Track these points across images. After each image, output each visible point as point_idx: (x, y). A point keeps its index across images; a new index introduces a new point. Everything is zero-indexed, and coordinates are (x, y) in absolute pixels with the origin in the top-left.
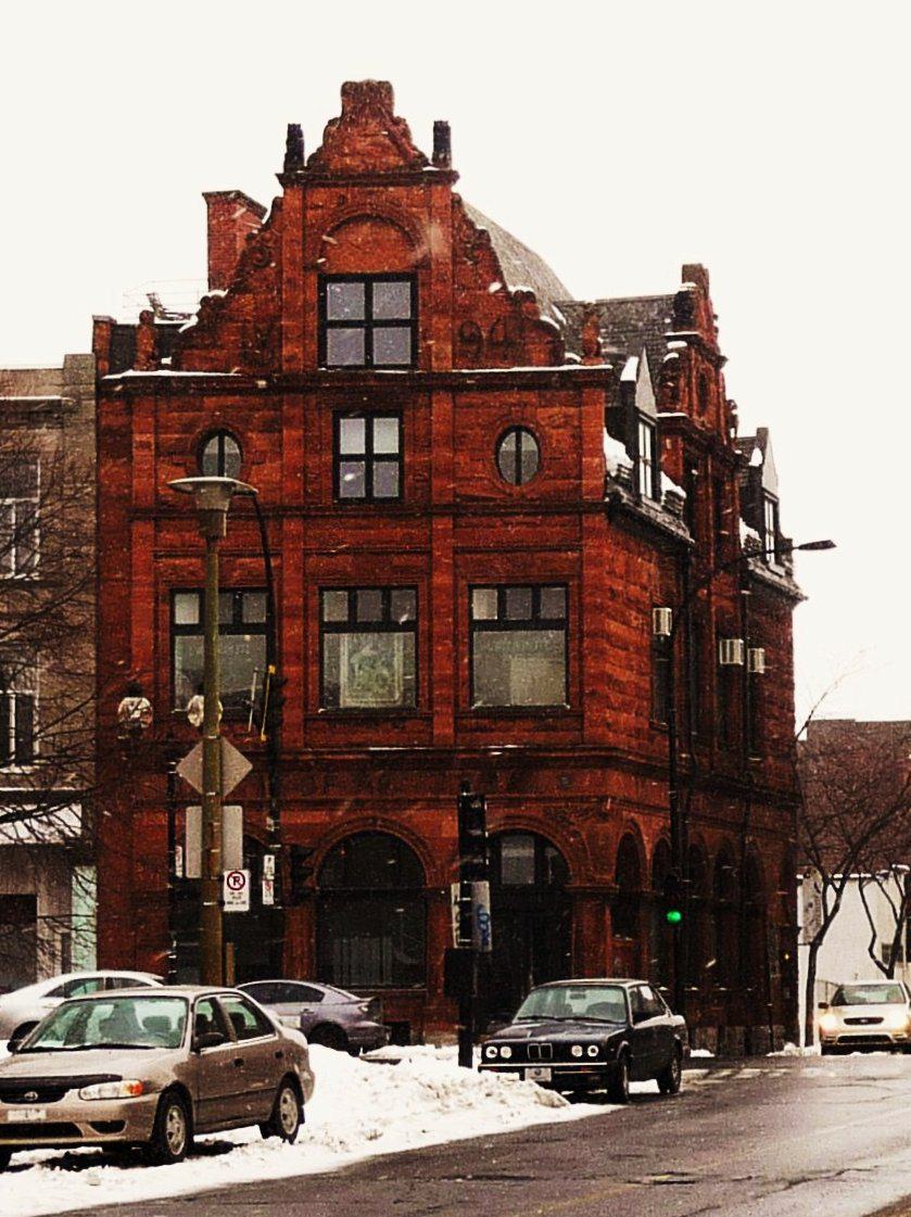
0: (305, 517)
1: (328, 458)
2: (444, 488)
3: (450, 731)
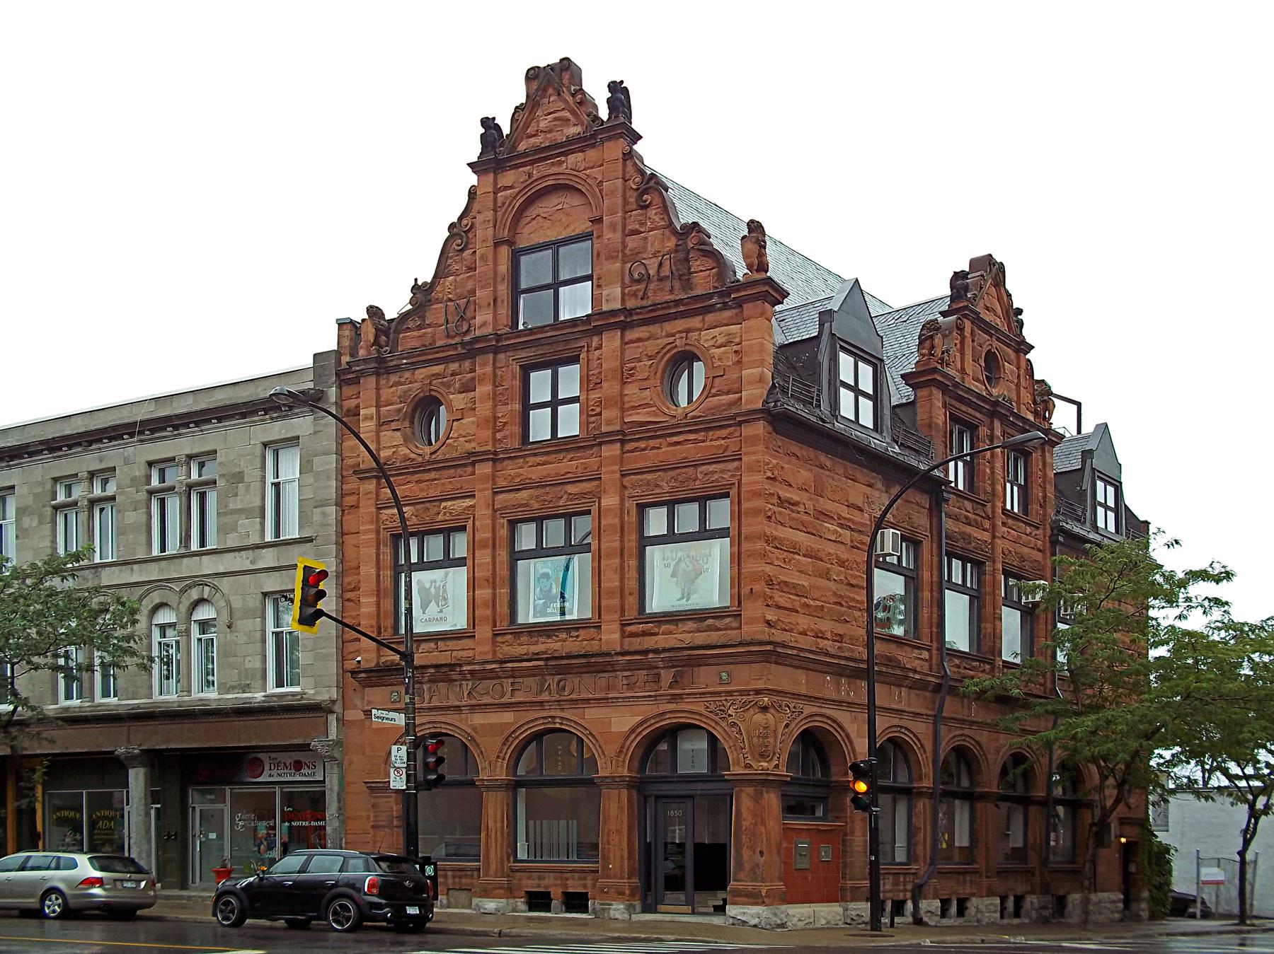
0: (494, 461)
1: (517, 407)
2: (610, 420)
3: (617, 636)
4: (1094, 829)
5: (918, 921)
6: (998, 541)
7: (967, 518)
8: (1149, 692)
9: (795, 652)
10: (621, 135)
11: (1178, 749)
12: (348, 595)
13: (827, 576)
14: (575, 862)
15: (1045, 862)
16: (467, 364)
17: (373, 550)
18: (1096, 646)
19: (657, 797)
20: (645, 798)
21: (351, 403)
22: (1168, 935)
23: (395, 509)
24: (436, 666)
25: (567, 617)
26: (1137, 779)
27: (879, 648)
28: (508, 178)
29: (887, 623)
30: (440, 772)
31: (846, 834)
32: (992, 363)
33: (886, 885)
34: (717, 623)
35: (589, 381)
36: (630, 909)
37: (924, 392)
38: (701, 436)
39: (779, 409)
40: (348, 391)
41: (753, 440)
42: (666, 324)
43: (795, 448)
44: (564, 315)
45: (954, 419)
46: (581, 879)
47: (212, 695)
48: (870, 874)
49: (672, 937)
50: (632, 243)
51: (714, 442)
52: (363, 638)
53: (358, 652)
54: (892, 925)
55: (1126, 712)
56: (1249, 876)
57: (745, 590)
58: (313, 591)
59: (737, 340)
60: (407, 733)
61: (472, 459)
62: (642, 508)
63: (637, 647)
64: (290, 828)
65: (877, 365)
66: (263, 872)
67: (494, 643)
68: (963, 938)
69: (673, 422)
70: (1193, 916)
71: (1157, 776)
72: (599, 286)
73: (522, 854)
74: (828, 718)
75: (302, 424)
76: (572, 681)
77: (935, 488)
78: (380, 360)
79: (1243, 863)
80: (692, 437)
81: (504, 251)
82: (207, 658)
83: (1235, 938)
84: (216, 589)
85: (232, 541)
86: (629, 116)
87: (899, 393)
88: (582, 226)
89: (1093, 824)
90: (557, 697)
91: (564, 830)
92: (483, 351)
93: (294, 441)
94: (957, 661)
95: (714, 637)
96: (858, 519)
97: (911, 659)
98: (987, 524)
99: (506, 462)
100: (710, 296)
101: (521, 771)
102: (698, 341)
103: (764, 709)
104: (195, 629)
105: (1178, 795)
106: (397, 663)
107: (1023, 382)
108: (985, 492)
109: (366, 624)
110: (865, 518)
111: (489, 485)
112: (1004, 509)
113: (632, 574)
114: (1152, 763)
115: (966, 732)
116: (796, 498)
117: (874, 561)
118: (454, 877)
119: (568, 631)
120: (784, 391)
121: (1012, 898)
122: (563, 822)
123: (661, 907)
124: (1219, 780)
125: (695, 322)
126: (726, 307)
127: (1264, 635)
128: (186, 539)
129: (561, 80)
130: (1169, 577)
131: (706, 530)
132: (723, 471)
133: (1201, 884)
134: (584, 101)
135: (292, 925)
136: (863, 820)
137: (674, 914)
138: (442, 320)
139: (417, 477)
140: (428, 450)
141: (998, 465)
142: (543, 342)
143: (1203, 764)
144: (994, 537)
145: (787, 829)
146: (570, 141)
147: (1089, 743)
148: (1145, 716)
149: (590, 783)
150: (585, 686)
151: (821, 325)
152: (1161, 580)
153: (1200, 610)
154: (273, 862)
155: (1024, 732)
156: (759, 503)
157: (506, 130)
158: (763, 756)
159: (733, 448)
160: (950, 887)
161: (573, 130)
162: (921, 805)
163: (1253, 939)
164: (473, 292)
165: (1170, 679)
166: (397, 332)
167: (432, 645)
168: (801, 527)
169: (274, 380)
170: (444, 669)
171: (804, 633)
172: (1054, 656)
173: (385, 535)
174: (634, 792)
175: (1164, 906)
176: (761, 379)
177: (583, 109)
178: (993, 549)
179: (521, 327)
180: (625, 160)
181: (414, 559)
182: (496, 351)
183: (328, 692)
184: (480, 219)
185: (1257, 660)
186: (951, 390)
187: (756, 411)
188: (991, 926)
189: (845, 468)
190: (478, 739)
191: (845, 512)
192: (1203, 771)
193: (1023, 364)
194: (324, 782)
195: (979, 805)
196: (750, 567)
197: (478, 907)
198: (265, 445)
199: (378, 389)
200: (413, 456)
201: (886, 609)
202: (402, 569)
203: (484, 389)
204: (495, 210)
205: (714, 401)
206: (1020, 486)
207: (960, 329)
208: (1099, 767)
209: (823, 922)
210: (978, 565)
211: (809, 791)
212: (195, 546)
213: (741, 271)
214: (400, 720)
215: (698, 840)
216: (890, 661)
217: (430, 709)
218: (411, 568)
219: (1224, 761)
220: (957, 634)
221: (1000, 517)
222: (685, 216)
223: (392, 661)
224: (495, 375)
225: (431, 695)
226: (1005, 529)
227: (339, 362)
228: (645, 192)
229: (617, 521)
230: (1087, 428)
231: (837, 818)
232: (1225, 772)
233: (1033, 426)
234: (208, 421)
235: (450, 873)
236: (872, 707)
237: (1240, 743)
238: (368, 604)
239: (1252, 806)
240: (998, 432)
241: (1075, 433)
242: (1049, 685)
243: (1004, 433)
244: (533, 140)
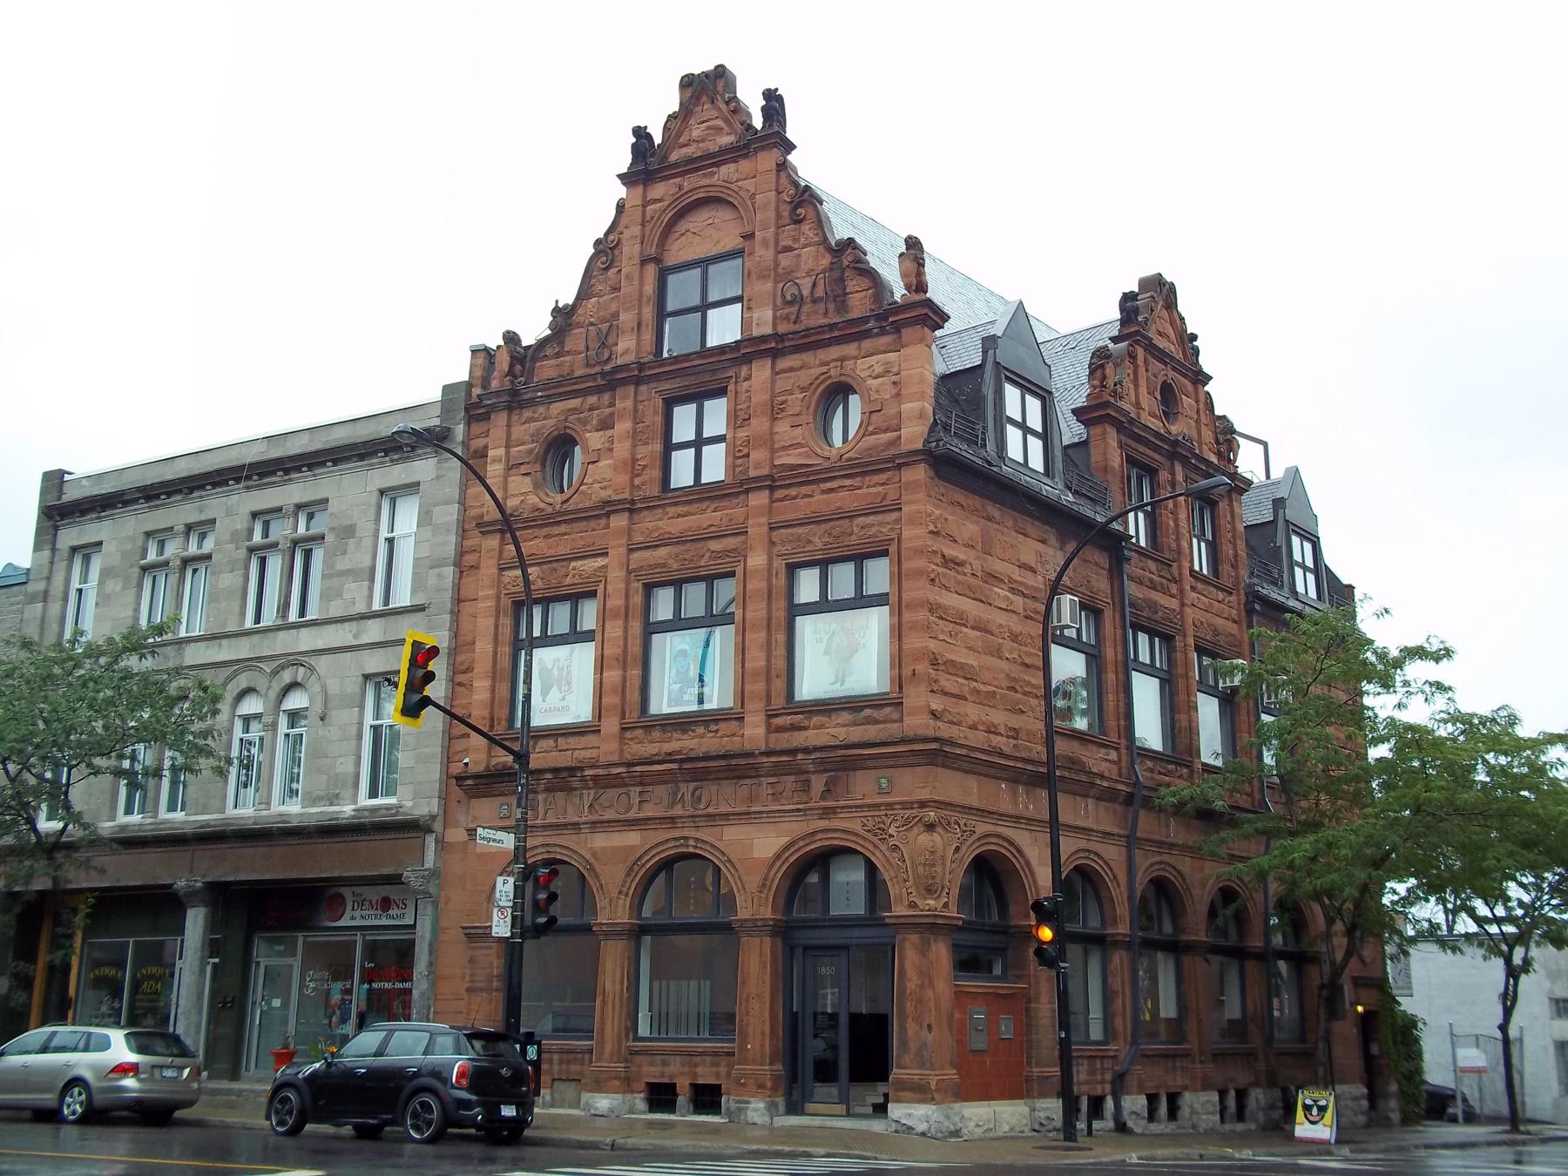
0: (631, 511)
1: (658, 447)
3: (761, 730)
4: (1325, 993)
5: (1121, 1127)
6: (1188, 610)
7: (1151, 581)
8: (1373, 804)
9: (964, 752)
10: (775, 145)
11: (1413, 881)
12: (460, 678)
13: (997, 652)
14: (706, 1040)
15: (1269, 1040)
16: (606, 397)
17: (492, 621)
18: (1308, 743)
19: (806, 948)
20: (792, 949)
21: (478, 443)
22: (1427, 1147)
23: (522, 573)
24: (555, 770)
25: (706, 706)
26: (1370, 924)
27: (1061, 746)
28: (659, 190)
29: (1068, 714)
30: (552, 913)
31: (1029, 1001)
32: (1168, 395)
33: (1080, 1073)
34: (876, 714)
35: (736, 416)
36: (772, 1108)
37: (1097, 430)
38: (856, 482)
39: (941, 451)
40: (477, 428)
41: (915, 485)
42: (819, 351)
43: (959, 495)
44: (712, 341)
45: (1131, 461)
46: (713, 1064)
47: (294, 808)
48: (1061, 1057)
49: (822, 1151)
50: (786, 260)
51: (871, 489)
52: (473, 733)
53: (466, 751)
54: (1090, 1133)
55: (1350, 831)
56: (1515, 1060)
57: (907, 672)
58: (420, 672)
59: (895, 370)
60: (516, 859)
61: (607, 509)
62: (792, 569)
63: (784, 745)
64: (370, 991)
65: (1045, 396)
66: (333, 1054)
67: (622, 739)
68: (1177, 1151)
69: (826, 465)
70: (1453, 1120)
71: (1392, 918)
72: (749, 308)
73: (644, 1030)
74: (1005, 839)
75: (423, 468)
76: (710, 790)
77: (1114, 544)
78: (514, 393)
79: (1506, 1042)
80: (847, 482)
81: (651, 270)
82: (293, 760)
83: (1507, 1153)
84: (312, 669)
85: (335, 610)
86: (783, 124)
87: (1071, 431)
88: (732, 241)
89: (1322, 986)
90: (691, 811)
91: (693, 994)
92: (624, 382)
93: (412, 488)
94: (1149, 764)
95: (872, 732)
96: (1031, 583)
97: (1098, 761)
98: (1174, 589)
99: (645, 513)
100: (865, 320)
101: (647, 912)
102: (854, 370)
103: (930, 827)
104: (283, 722)
105: (1420, 946)
106: (509, 766)
108: (1171, 550)
109: (478, 716)
110: (1038, 582)
111: (624, 541)
112: (1192, 570)
113: (780, 651)
114: (1386, 900)
115: (1165, 858)
116: (962, 557)
117: (1051, 636)
118: (561, 1062)
119: (706, 723)
120: (946, 428)
121: (1232, 1093)
122: (693, 983)
123: (810, 1107)
124: (1465, 925)
125: (850, 349)
126: (883, 332)
127: (1497, 729)
128: (284, 607)
129: (715, 86)
130: (1382, 656)
131: (863, 597)
132: (881, 524)
133: (1460, 1072)
134: (737, 109)
135: (364, 1133)
136: (1049, 980)
137: (824, 1118)
138: (582, 347)
139: (545, 531)
140: (559, 498)
141: (1183, 516)
142: (690, 371)
143: (1443, 901)
144: (1183, 605)
145: (960, 995)
146: (724, 151)
147: (1309, 873)
148: (1370, 836)
149: (726, 928)
151: (985, 352)
152: (1373, 659)
153: (1421, 697)
154: (345, 1040)
155: (1233, 858)
156: (920, 563)
157: (658, 140)
158: (930, 891)
159: (893, 495)
160: (1158, 1077)
161: (726, 140)
162: (1118, 959)
163: (1530, 1153)
164: (616, 315)
165: (1395, 787)
166: (534, 360)
167: (551, 742)
168: (968, 592)
169: (399, 416)
170: (564, 774)
171: (974, 727)
172: (1260, 757)
173: (506, 602)
174: (779, 942)
175: (1417, 1104)
176: (921, 415)
177: (737, 117)
178: (1182, 619)
179: (665, 355)
180: (778, 171)
181: (537, 633)
182: (638, 381)
183: (429, 804)
184: (627, 234)
185: (1493, 761)
186: (1127, 428)
187: (916, 452)
188: (1210, 1135)
189: (1015, 520)
190: (598, 869)
191: (1017, 574)
192: (1446, 911)
193: (1202, 398)
194: (414, 926)
195: (1187, 959)
196: (914, 642)
197: (588, 1106)
198: (382, 492)
199: (509, 426)
200: (542, 505)
201: (1067, 695)
202: (523, 645)
203: (623, 426)
204: (643, 225)
205: (871, 440)
206: (1207, 542)
207: (1133, 357)
208: (1323, 906)
209: (1006, 1128)
210: (1167, 639)
211: (983, 939)
212: (293, 616)
213: (899, 291)
214: (508, 841)
215: (854, 1010)
216: (1074, 763)
217: (545, 827)
218: (534, 643)
219: (1469, 898)
220: (1149, 728)
221: (1188, 582)
222: (840, 232)
223: (504, 764)
224: (636, 410)
225: (550, 809)
226: (1194, 595)
227: (469, 394)
229: (764, 584)
230: (1277, 473)
231: (1019, 978)
232: (1472, 913)
233: (1218, 469)
234: (322, 464)
235: (556, 1057)
236: (1054, 826)
237: (1484, 873)
238: (481, 690)
239: (1508, 961)
240: (1180, 477)
241: (1263, 478)
242: (1257, 796)
243: (1186, 478)
244: (684, 150)
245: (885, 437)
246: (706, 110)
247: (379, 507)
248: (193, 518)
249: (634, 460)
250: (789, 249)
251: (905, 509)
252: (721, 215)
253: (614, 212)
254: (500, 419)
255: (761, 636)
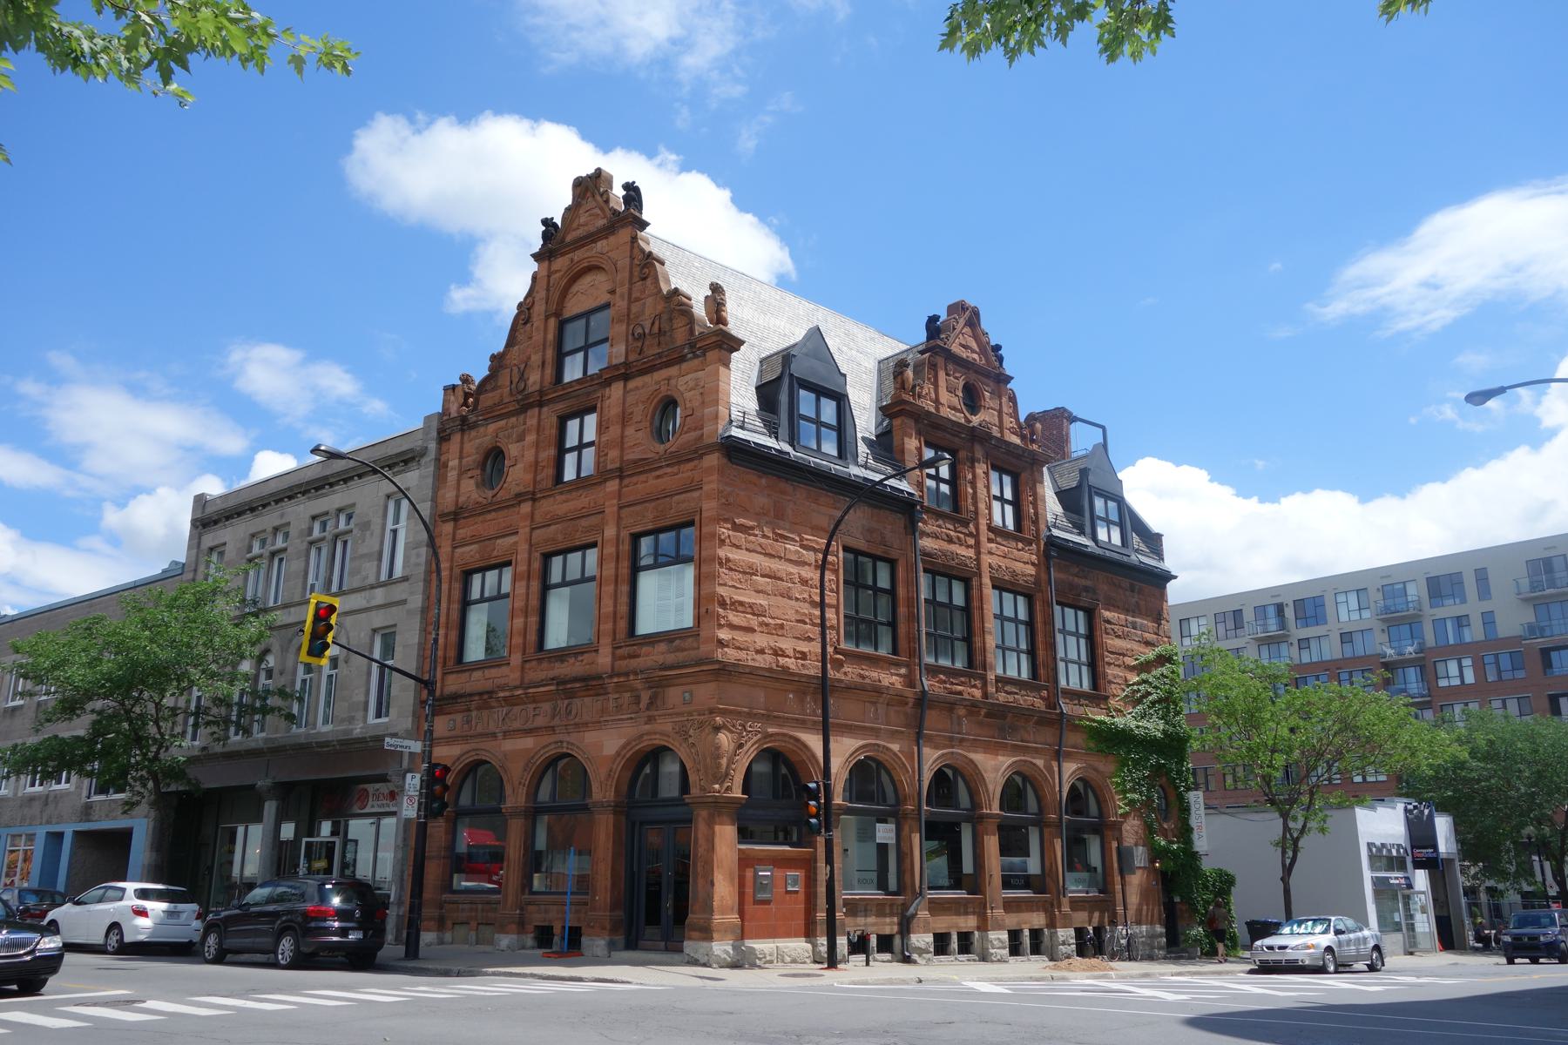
1: (552, 452)
3: (608, 660)
24: (481, 694)
28: (561, 263)
38: (675, 469)
61: (519, 498)
80: (669, 470)
81: (552, 322)
86: (640, 208)
107: (1005, 409)
113: (624, 599)
125: (673, 371)
126: (696, 357)
146: (599, 231)
150: (586, 706)
161: (601, 222)
182: (541, 404)
199: (462, 443)
228: (645, 266)
245: (693, 435)
246: (590, 203)
247: (386, 508)
248: (277, 523)
249: (537, 462)
250: (638, 299)
251: (705, 488)
252: (599, 278)
253: (529, 282)
254: (456, 438)
255: (611, 588)
